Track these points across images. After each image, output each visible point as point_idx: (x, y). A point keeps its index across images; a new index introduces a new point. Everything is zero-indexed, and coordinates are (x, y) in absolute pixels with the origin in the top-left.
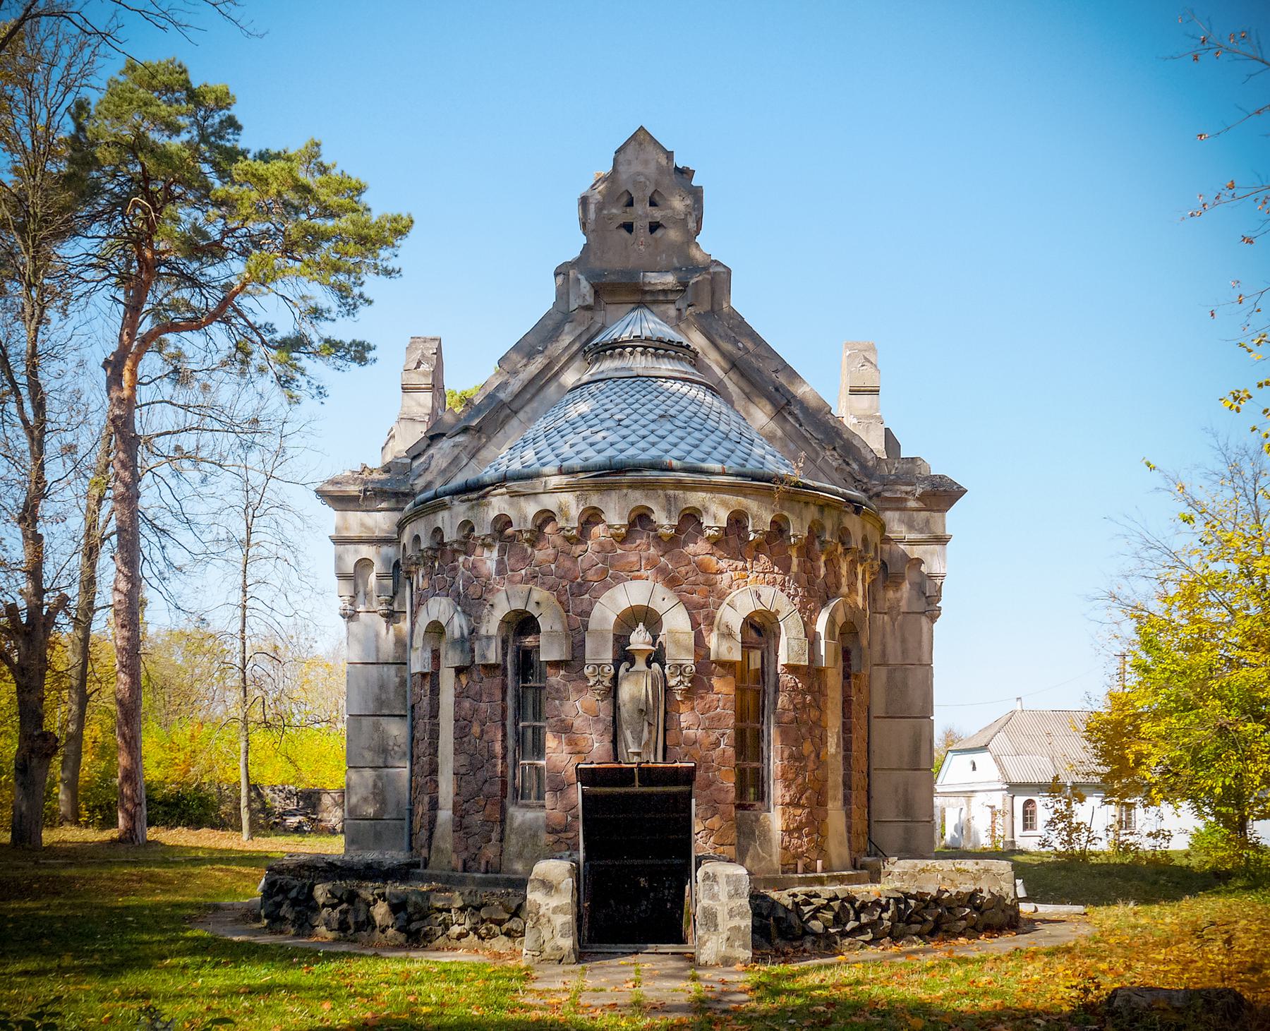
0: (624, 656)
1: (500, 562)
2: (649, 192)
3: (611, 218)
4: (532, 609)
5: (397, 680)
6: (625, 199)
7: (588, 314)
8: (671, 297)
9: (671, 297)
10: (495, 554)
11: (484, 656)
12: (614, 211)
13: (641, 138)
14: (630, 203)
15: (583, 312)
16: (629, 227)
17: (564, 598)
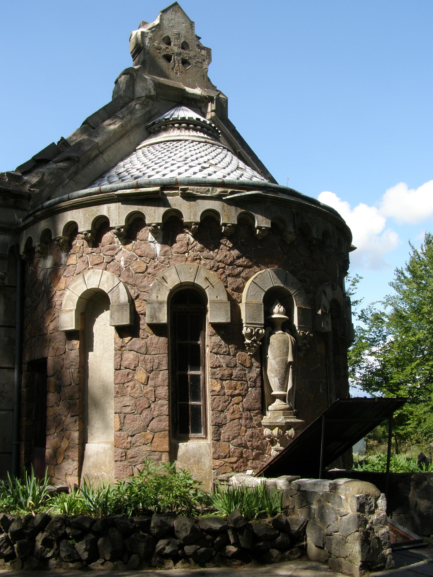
4: (200, 282)
14: (169, 43)
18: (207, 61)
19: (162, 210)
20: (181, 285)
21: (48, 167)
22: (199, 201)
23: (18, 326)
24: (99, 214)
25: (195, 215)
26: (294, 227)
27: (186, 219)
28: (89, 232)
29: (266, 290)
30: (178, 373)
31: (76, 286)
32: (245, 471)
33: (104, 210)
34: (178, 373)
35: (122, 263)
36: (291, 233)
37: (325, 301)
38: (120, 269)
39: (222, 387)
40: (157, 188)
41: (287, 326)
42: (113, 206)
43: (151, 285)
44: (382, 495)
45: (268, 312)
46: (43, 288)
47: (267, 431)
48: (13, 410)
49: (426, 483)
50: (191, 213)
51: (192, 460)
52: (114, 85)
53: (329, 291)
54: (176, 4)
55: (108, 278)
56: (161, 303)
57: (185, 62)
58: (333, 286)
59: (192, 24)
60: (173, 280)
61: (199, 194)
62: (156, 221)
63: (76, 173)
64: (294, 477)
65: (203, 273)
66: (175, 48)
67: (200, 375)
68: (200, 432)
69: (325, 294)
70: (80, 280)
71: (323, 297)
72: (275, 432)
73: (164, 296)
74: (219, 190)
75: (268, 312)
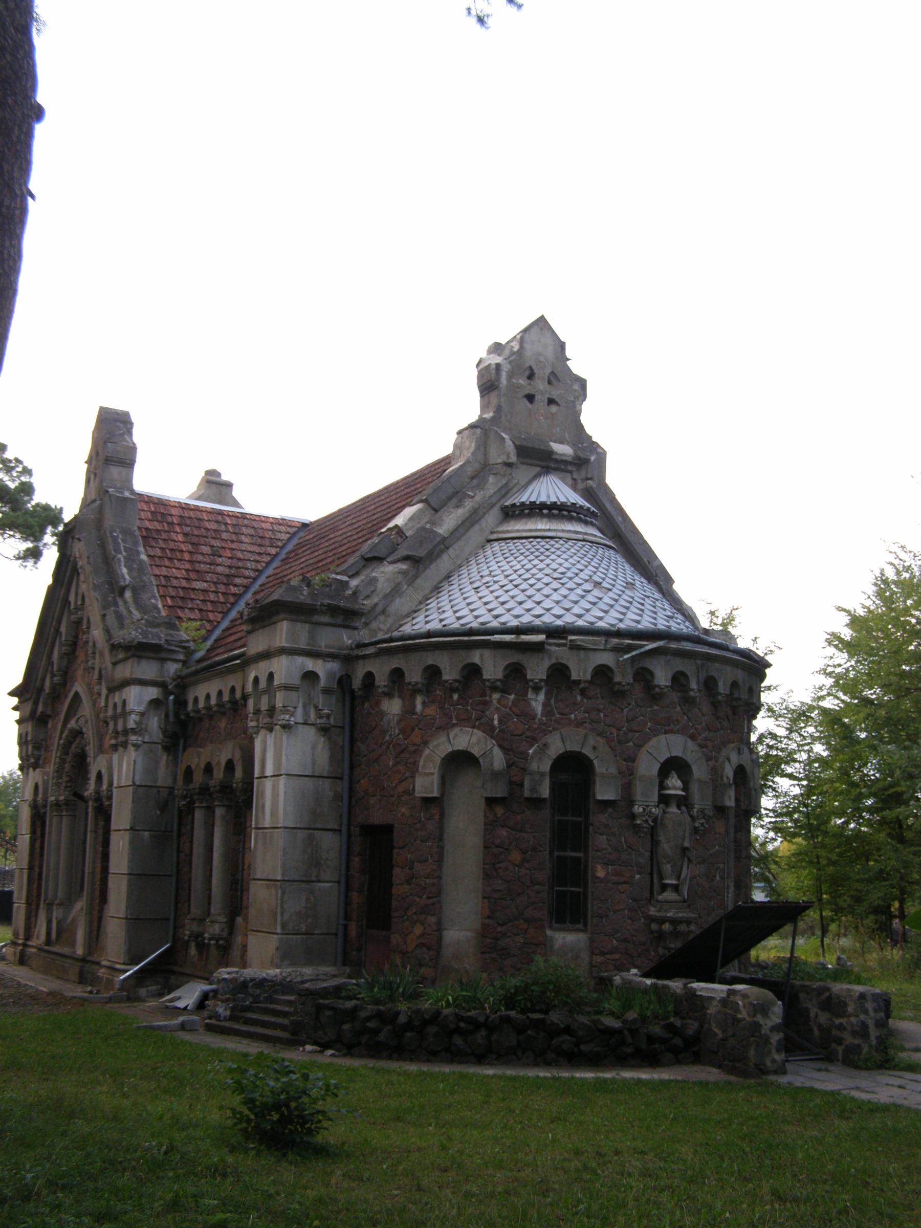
0: (664, 800)
1: (545, 705)
2: (548, 371)
3: (519, 387)
4: (587, 751)
5: (331, 794)
6: (527, 373)
7: (509, 470)
8: (570, 468)
9: (570, 468)
10: (541, 697)
11: (533, 789)
12: (521, 381)
13: (541, 324)
14: (531, 377)
15: (505, 468)
16: (530, 398)
17: (613, 744)
18: (581, 399)
19: (546, 664)
20: (566, 752)
21: (382, 569)
22: (591, 654)
23: (346, 778)
24: (469, 661)
25: (585, 673)
26: (698, 683)
27: (574, 677)
29: (662, 761)
30: (556, 854)
31: (438, 745)
32: (628, 971)
33: (476, 657)
34: (556, 854)
35: (496, 722)
36: (693, 690)
37: (729, 772)
38: (493, 728)
39: (608, 873)
40: (542, 637)
41: (684, 802)
42: (487, 653)
43: (531, 751)
44: (780, 1003)
45: (662, 787)
46: (387, 738)
47: (654, 926)
48: (339, 882)
49: (827, 994)
50: (581, 670)
51: (570, 955)
52: (456, 436)
53: (734, 757)
54: (542, 317)
55: (479, 741)
56: (542, 774)
57: (551, 401)
58: (739, 749)
59: (562, 345)
60: (556, 746)
61: (590, 646)
62: (540, 677)
63: (416, 577)
64: (689, 980)
65: (591, 741)
66: (540, 385)
67: (580, 858)
68: (579, 922)
69: (729, 760)
70: (443, 739)
71: (727, 764)
72: (666, 927)
73: (546, 766)
74: (615, 641)
75: (662, 787)
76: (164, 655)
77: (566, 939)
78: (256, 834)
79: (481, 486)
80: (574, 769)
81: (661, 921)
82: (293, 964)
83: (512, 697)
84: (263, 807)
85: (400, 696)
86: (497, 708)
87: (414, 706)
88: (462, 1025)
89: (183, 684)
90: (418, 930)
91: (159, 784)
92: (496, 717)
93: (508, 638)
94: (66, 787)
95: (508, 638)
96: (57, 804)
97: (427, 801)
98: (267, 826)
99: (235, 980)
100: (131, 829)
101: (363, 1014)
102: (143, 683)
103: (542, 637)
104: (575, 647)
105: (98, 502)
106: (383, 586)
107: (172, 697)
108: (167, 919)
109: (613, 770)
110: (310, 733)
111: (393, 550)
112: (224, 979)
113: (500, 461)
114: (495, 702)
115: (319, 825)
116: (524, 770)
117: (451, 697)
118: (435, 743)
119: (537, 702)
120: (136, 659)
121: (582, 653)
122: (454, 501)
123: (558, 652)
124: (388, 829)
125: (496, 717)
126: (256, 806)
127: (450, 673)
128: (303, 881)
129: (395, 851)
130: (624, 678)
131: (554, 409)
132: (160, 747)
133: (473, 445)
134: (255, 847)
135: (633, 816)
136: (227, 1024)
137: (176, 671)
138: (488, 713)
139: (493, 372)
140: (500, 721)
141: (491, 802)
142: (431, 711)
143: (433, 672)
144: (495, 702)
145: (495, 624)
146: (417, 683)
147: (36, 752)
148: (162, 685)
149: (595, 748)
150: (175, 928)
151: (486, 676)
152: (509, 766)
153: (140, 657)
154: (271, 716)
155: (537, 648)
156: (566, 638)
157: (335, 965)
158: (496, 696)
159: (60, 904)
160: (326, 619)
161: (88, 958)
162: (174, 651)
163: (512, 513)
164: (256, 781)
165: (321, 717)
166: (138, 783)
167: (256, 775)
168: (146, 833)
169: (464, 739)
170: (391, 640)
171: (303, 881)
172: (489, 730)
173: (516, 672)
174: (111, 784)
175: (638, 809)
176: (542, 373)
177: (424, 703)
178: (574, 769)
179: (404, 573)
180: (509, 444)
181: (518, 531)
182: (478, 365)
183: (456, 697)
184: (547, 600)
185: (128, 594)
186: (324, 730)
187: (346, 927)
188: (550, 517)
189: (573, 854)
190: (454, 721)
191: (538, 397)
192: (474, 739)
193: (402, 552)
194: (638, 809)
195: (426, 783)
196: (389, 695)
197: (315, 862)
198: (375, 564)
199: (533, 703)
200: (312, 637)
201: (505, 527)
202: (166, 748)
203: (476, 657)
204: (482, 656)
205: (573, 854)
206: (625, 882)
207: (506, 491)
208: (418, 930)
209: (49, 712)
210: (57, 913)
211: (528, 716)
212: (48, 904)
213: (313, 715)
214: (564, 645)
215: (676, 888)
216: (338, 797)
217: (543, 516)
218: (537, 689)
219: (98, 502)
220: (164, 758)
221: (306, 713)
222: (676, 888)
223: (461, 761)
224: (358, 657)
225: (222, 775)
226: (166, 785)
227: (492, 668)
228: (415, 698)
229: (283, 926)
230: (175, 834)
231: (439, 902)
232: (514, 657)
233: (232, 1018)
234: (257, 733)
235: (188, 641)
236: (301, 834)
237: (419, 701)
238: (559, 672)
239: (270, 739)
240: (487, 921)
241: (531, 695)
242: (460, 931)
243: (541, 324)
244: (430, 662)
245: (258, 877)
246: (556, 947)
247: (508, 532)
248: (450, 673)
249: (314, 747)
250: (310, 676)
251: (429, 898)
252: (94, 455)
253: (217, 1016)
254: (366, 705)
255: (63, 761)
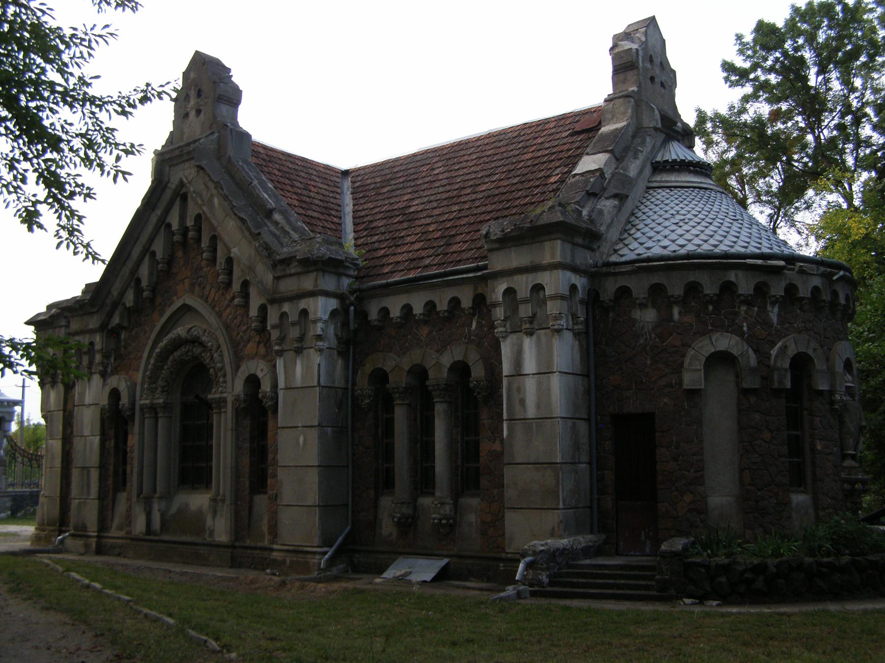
1: (779, 315)
10: (776, 310)
13: (651, 22)
19: (783, 284)
24: (726, 279)
28: (715, 295)
33: (732, 276)
35: (745, 329)
40: (782, 263)
42: (740, 273)
46: (642, 341)
47: (846, 486)
56: (786, 370)
59: (664, 41)
73: (787, 364)
74: (822, 269)
76: (341, 270)
77: (799, 499)
78: (508, 424)
79: (643, 143)
80: (801, 365)
81: (853, 482)
82: (570, 535)
83: (756, 309)
84: (522, 402)
85: (654, 307)
86: (745, 318)
87: (671, 315)
88: (825, 570)
89: (362, 296)
90: (688, 498)
91: (336, 385)
92: (745, 324)
93: (759, 262)
94: (163, 391)
95: (759, 262)
96: (153, 409)
97: (693, 393)
98: (530, 417)
99: (549, 550)
100: (319, 425)
101: (740, 568)
102: (327, 294)
103: (782, 263)
104: (802, 272)
105: (216, 135)
106: (607, 218)
107: (352, 308)
108: (347, 505)
109: (825, 367)
110: (568, 336)
111: (604, 189)
112: (541, 551)
113: (651, 125)
114: (743, 312)
115: (578, 416)
116: (769, 366)
117: (707, 308)
118: (700, 345)
119: (774, 314)
120: (321, 274)
121: (804, 276)
122: (631, 154)
123: (791, 275)
124: (649, 417)
125: (745, 324)
126: (508, 398)
127: (710, 288)
128: (571, 463)
129: (657, 434)
130: (826, 297)
131: (663, 90)
132: (336, 352)
133: (630, 111)
134: (509, 435)
135: (832, 403)
136: (549, 589)
137: (350, 286)
138: (737, 321)
139: (635, 55)
140: (749, 328)
141: (745, 392)
142: (689, 319)
143: (693, 288)
144: (743, 312)
145: (683, 251)
146: (679, 296)
147: (105, 361)
148: (341, 297)
149: (815, 350)
150: (353, 511)
151: (741, 291)
152: (759, 363)
153: (324, 271)
154: (531, 323)
155: (777, 270)
156: (794, 265)
157: (591, 532)
158: (744, 308)
159: (160, 498)
160: (579, 240)
161: (237, 544)
162: (348, 267)
163: (660, 167)
164: (505, 382)
165: (577, 324)
166: (322, 384)
167: (504, 374)
168: (329, 429)
169: (725, 342)
170: (649, 260)
171: (571, 463)
172: (741, 334)
173: (761, 290)
174: (275, 386)
175: (838, 397)
176: (657, 61)
177: (680, 313)
178: (801, 365)
179: (615, 207)
180: (657, 112)
181: (677, 182)
182: (611, 49)
183: (711, 308)
184: (681, 239)
185: (277, 217)
186: (576, 335)
187: (598, 500)
188: (696, 173)
189: (794, 433)
190: (710, 328)
191: (656, 80)
192: (733, 342)
193: (612, 191)
194: (838, 397)
195: (692, 376)
196: (643, 306)
197: (576, 446)
198: (592, 199)
199: (771, 314)
200: (573, 256)
201: (658, 179)
202: (340, 353)
203: (732, 276)
204: (736, 275)
205: (794, 433)
206: (831, 454)
207: (654, 151)
208: (688, 498)
209: (125, 324)
210: (156, 506)
211: (767, 324)
212: (146, 498)
213: (571, 322)
214: (793, 269)
215: (853, 457)
216: (588, 392)
217: (690, 172)
218: (773, 304)
219: (216, 135)
220: (340, 363)
221: (567, 321)
222: (853, 457)
223: (720, 360)
224: (608, 274)
225: (446, 375)
226: (341, 386)
227: (745, 285)
228: (671, 308)
229: (564, 504)
230: (350, 430)
231: (702, 476)
232: (762, 278)
233: (551, 584)
234: (505, 338)
235: (357, 259)
236: (570, 422)
237: (676, 311)
238: (791, 289)
239: (528, 343)
240: (749, 487)
241: (769, 308)
242: (721, 495)
243: (651, 22)
244: (692, 279)
245: (519, 460)
246: (794, 505)
247: (667, 182)
248: (710, 288)
249: (572, 349)
250: (573, 288)
251: (697, 471)
252: (193, 93)
253: (540, 583)
254: (611, 315)
255: (158, 368)
